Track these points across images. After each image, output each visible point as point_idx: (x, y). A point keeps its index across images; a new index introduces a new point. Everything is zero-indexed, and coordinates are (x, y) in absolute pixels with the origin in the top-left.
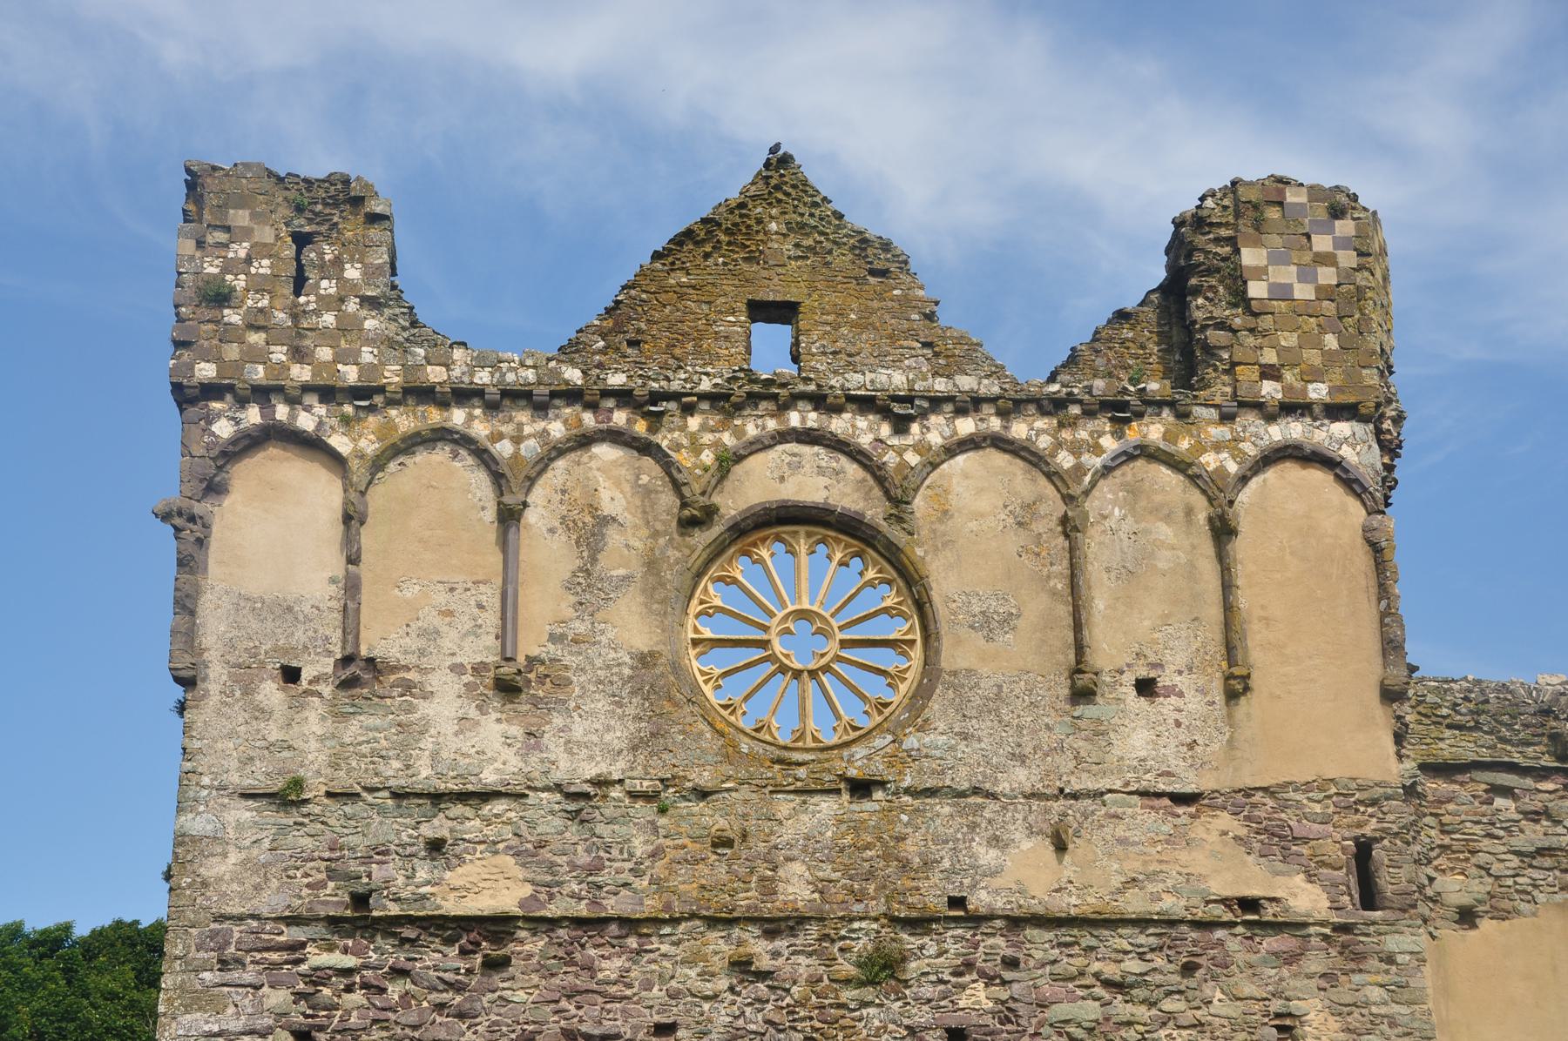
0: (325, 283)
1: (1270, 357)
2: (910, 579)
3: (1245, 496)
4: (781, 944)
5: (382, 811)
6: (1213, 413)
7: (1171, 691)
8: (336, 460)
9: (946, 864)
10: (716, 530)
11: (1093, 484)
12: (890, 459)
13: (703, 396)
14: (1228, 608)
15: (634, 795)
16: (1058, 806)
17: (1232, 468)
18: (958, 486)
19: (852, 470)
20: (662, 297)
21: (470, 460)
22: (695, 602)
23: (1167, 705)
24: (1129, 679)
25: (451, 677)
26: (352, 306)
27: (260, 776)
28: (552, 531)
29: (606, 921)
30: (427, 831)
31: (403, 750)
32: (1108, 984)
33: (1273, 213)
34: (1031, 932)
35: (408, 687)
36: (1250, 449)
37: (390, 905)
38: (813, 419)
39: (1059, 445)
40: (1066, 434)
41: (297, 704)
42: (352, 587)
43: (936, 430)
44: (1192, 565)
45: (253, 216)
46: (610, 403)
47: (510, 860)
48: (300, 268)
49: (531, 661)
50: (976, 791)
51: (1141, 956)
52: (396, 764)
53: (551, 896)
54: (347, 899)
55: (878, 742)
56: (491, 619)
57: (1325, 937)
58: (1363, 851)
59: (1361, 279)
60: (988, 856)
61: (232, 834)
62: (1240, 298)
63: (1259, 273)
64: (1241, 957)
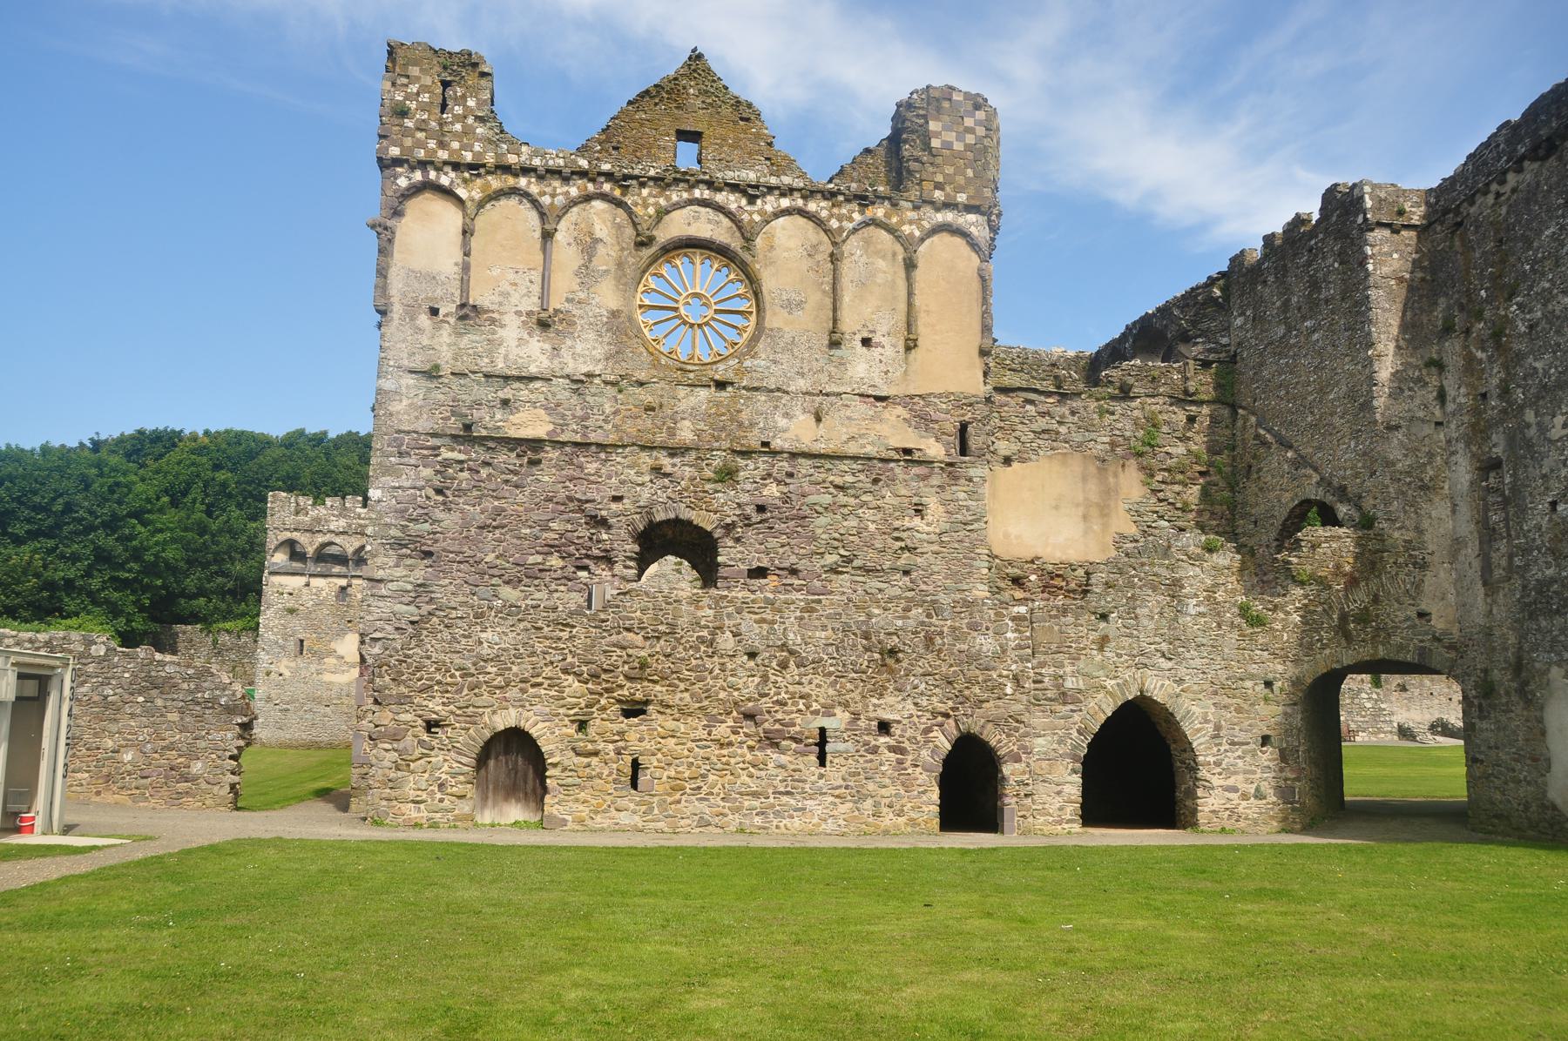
0: (456, 108)
1: (940, 178)
2: (752, 280)
3: (922, 249)
4: (677, 460)
5: (479, 383)
6: (910, 205)
7: (879, 345)
8: (460, 201)
9: (761, 425)
10: (653, 249)
11: (848, 237)
12: (746, 217)
13: (650, 178)
14: (910, 305)
15: (606, 383)
16: (819, 399)
17: (917, 233)
18: (779, 234)
19: (726, 222)
20: (632, 125)
21: (528, 205)
22: (641, 285)
23: (875, 352)
24: (858, 337)
25: (515, 317)
26: (470, 120)
27: (418, 362)
28: (569, 244)
29: (590, 444)
30: (501, 394)
31: (490, 353)
32: (836, 487)
33: (946, 104)
34: (801, 460)
35: (493, 321)
36: (926, 225)
37: (482, 430)
38: (707, 194)
39: (832, 216)
40: (835, 210)
41: (437, 327)
42: (466, 268)
43: (770, 204)
44: (894, 281)
45: (421, 70)
46: (602, 179)
47: (543, 412)
48: (444, 99)
49: (556, 311)
50: (778, 390)
51: (853, 474)
52: (486, 360)
53: (563, 431)
54: (461, 426)
55: (731, 363)
56: (536, 289)
57: (942, 468)
58: (963, 428)
59: (986, 142)
60: (782, 422)
61: (404, 390)
62: (927, 147)
63: (937, 135)
64: (901, 477)
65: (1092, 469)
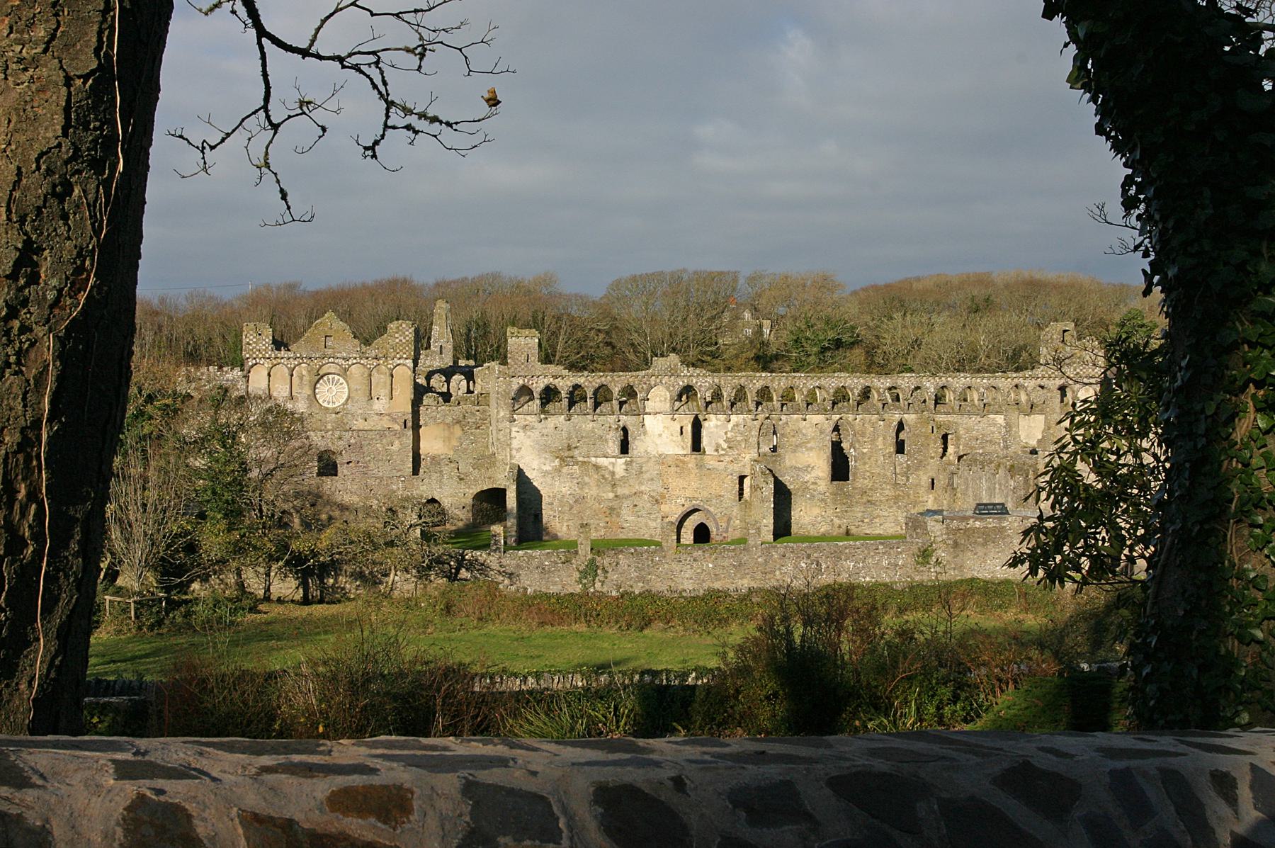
18: (353, 370)
56: (288, 390)
58: (405, 421)
60: (355, 422)
65: (446, 427)
